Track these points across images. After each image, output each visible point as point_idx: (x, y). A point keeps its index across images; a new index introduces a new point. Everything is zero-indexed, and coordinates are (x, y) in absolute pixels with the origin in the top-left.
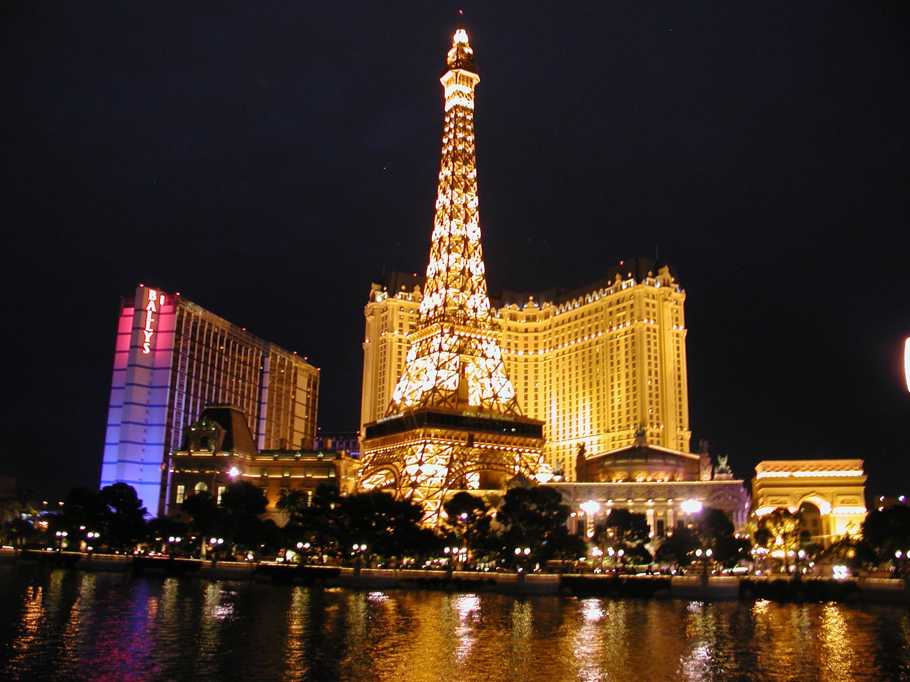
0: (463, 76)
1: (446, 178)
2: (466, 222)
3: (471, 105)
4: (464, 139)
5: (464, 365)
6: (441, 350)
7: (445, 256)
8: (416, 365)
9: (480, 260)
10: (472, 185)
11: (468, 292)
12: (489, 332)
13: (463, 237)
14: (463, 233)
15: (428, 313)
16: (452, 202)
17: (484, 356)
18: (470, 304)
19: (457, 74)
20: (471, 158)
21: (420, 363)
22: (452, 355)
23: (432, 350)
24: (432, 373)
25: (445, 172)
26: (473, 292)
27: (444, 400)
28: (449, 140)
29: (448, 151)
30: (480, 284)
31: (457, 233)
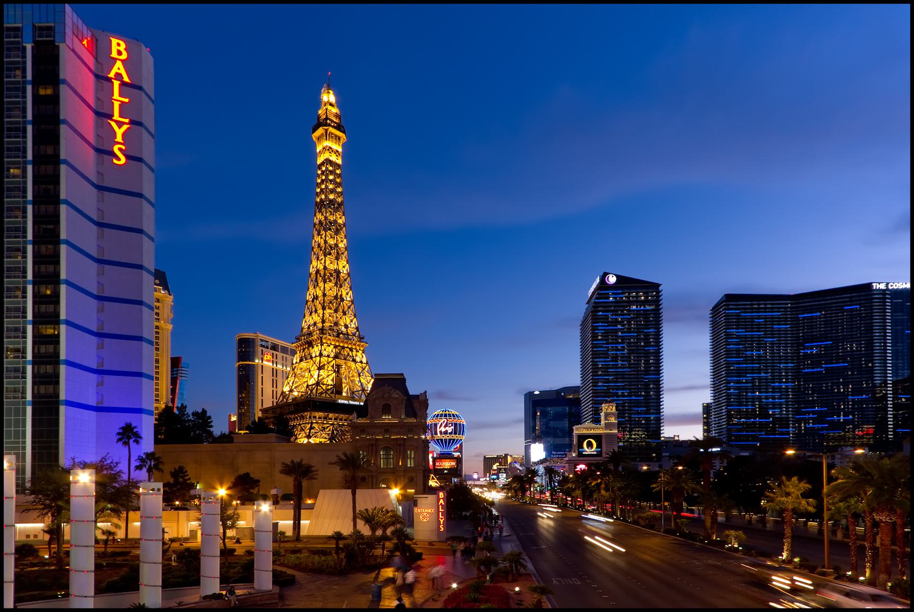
1: (320, 221)
2: (337, 259)
5: (339, 366)
6: (321, 355)
7: (321, 284)
8: (300, 366)
11: (340, 313)
15: (309, 328)
16: (326, 242)
21: (303, 365)
22: (330, 359)
24: (315, 373)
26: (344, 313)
28: (322, 190)
29: (321, 199)
31: (332, 267)
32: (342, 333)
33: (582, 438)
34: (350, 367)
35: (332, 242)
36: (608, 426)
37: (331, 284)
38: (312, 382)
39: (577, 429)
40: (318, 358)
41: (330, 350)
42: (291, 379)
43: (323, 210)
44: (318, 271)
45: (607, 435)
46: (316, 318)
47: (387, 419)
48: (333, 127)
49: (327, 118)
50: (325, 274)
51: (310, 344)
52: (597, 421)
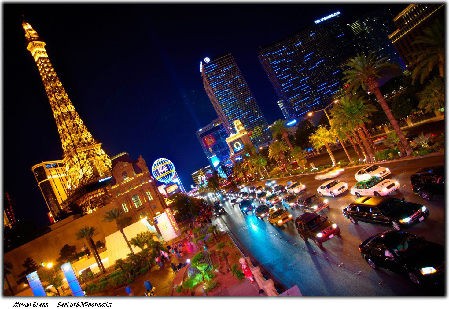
0: (37, 44)
2: (66, 105)
3: (46, 56)
4: (50, 72)
5: (92, 162)
7: (63, 122)
9: (79, 118)
10: (62, 89)
11: (80, 133)
12: (96, 145)
13: (68, 112)
14: (67, 110)
16: (56, 99)
17: (98, 155)
18: (83, 138)
19: (33, 43)
20: (57, 78)
21: (73, 169)
22: (85, 160)
23: (75, 162)
24: (80, 171)
25: (48, 88)
26: (82, 132)
27: (90, 179)
28: (43, 74)
29: (45, 79)
30: (83, 128)
31: (65, 111)
32: (85, 143)
33: (232, 143)
34: (97, 160)
35: (59, 98)
36: (241, 132)
37: (69, 120)
38: (81, 177)
39: (228, 140)
40: (78, 163)
41: (83, 155)
42: (69, 180)
43: (48, 83)
44: (59, 116)
45: (243, 137)
46: (68, 141)
47: (127, 180)
48: (36, 40)
49: (31, 37)
50: (63, 116)
51: (71, 157)
52: (235, 132)
